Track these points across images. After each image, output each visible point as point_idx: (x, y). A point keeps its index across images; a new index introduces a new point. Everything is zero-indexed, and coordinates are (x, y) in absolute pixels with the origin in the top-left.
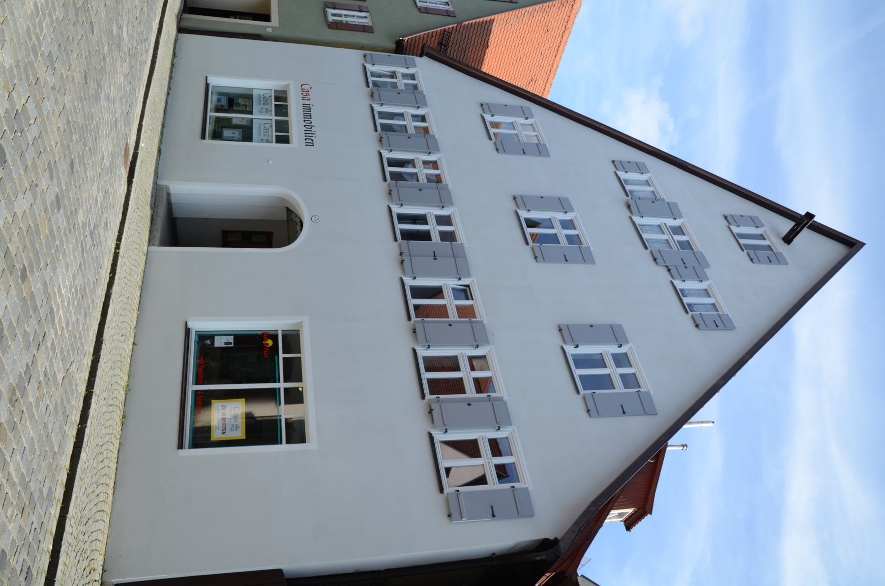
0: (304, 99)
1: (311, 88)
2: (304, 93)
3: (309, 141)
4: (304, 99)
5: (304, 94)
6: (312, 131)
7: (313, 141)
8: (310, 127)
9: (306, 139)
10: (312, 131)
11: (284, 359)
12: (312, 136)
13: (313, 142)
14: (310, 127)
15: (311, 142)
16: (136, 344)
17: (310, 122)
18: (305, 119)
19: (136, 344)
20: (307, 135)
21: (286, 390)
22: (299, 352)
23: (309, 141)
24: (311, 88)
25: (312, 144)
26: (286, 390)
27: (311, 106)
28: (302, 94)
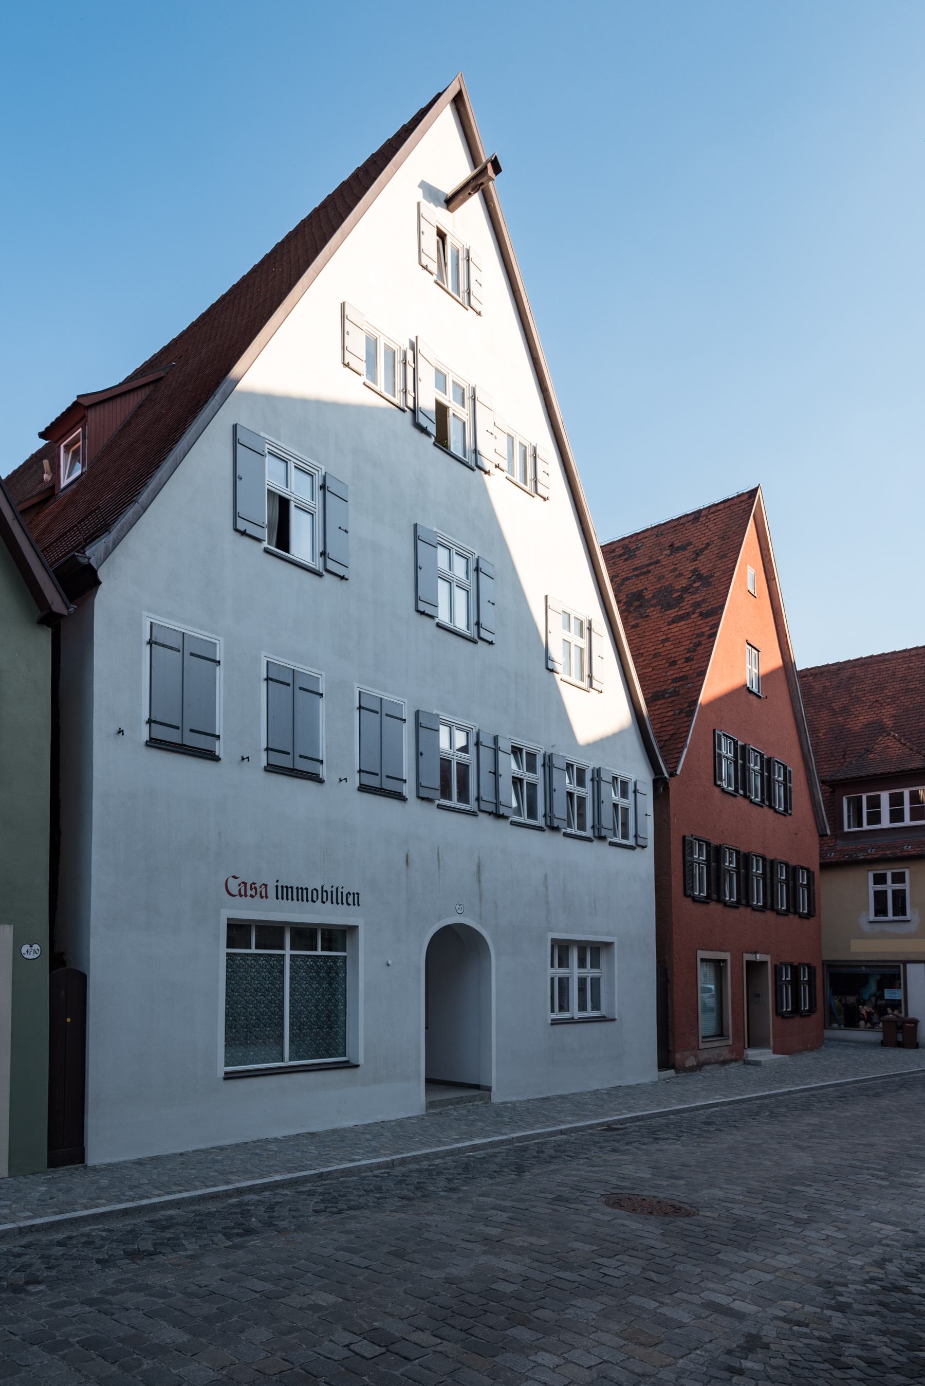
0: (264, 894)
1: (234, 877)
2: (249, 892)
3: (353, 899)
4: (264, 894)
5: (253, 893)
6: (332, 892)
7: (349, 893)
8: (325, 893)
9: (349, 904)
10: (332, 892)
11: (257, 948)
12: (342, 893)
13: (352, 893)
14: (325, 893)
15: (352, 895)
16: (242, 757)
17: (315, 892)
18: (310, 898)
19: (242, 757)
20: (340, 901)
21: (283, 956)
22: (910, 807)
23: (353, 899)
24: (234, 877)
25: (356, 896)
26: (283, 956)
27: (280, 885)
28: (252, 896)
